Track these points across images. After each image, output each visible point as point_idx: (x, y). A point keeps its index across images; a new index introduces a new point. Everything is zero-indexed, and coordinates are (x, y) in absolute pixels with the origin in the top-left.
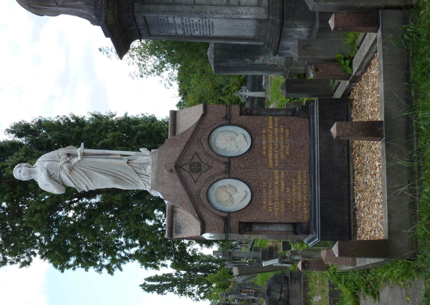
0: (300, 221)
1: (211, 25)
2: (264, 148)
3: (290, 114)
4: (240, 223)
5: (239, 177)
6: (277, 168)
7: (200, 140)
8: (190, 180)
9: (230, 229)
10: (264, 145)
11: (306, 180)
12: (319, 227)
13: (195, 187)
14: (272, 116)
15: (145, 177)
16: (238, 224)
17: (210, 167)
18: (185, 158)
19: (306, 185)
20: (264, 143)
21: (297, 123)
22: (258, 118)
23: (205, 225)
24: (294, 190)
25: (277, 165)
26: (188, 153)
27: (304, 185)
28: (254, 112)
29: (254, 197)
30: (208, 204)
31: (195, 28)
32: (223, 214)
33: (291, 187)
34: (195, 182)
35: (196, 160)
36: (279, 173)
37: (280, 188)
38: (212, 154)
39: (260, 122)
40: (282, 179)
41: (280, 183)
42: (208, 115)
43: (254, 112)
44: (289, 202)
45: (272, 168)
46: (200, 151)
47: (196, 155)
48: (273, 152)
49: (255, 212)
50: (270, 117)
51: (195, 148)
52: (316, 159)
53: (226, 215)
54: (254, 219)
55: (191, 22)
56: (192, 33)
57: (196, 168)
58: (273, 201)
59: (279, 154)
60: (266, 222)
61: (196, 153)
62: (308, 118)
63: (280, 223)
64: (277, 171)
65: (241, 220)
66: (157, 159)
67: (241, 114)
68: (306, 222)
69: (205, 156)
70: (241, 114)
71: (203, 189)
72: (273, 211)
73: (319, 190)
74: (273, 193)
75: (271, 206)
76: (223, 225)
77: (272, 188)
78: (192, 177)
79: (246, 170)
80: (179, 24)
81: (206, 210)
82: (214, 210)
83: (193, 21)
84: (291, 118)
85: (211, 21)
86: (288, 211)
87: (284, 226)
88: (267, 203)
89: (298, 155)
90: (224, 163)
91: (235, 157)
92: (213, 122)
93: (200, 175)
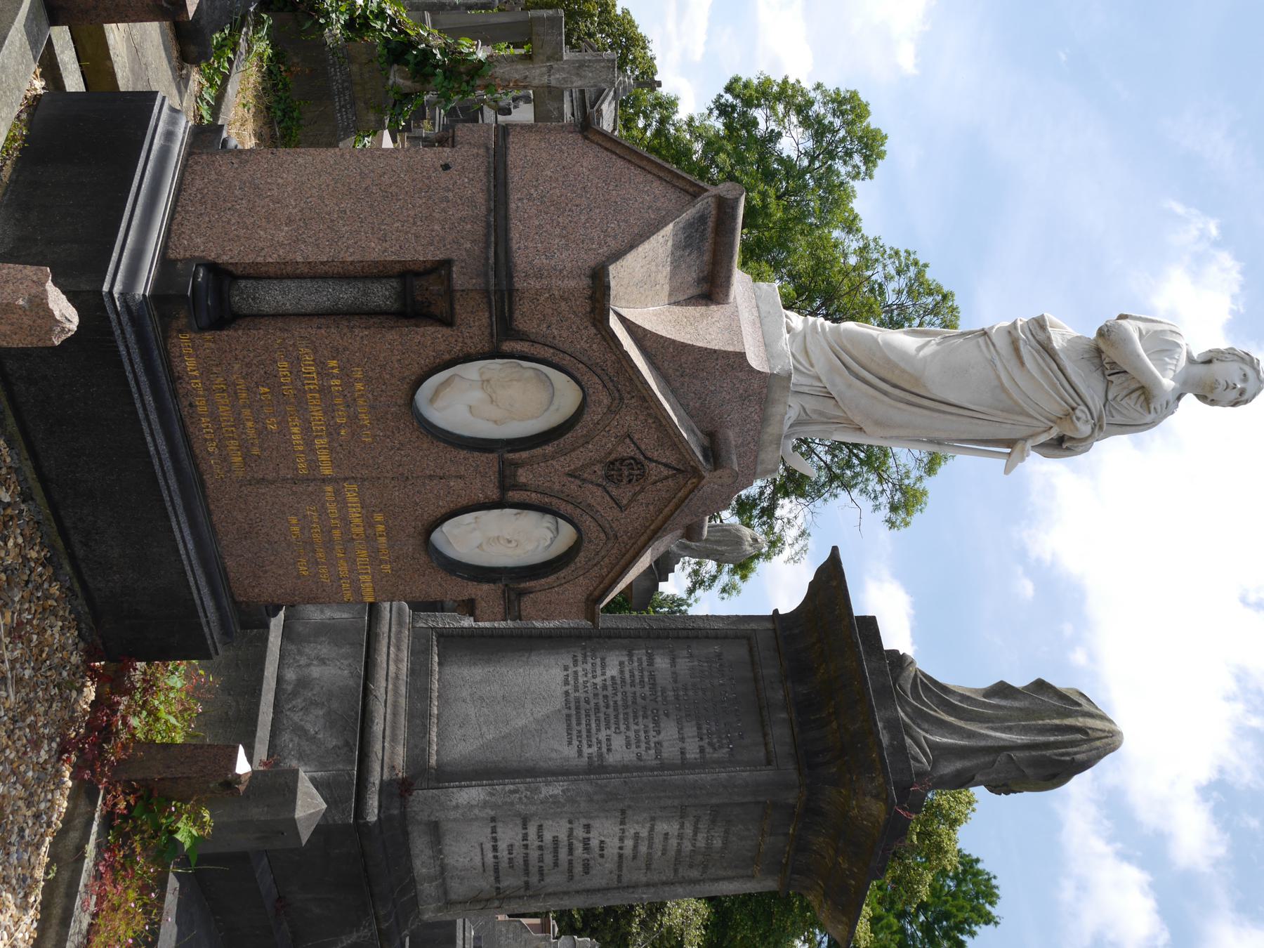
0: (208, 336)
1: (574, 722)
7: (608, 539)
9: (489, 302)
11: (209, 454)
12: (118, 332)
15: (806, 389)
16: (458, 321)
18: (664, 494)
19: (206, 440)
23: (593, 310)
24: (249, 424)
25: (329, 489)
26: (651, 507)
27: (212, 440)
30: (579, 376)
31: (619, 698)
32: (519, 346)
33: (262, 432)
36: (314, 465)
39: (401, 588)
40: (302, 452)
41: (309, 444)
44: (263, 390)
47: (625, 502)
48: (346, 521)
49: (394, 359)
52: (183, 518)
53: (507, 346)
55: (632, 734)
56: (625, 659)
58: (324, 391)
62: (235, 602)
64: (327, 472)
66: (762, 456)
68: (180, 331)
69: (592, 501)
71: (596, 418)
72: (321, 365)
73: (149, 439)
74: (329, 410)
76: (517, 314)
77: (332, 432)
78: (638, 448)
80: (667, 715)
81: (585, 359)
82: (555, 360)
83: (628, 745)
85: (575, 743)
87: (266, 308)
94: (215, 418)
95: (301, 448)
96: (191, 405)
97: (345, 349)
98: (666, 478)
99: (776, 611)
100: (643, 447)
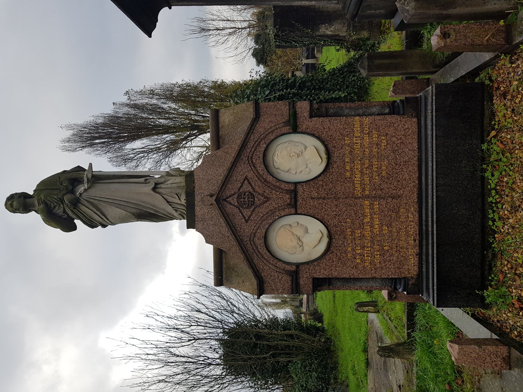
2: (348, 168)
3: (387, 111)
4: (314, 279)
5: (311, 212)
6: (368, 197)
7: (251, 158)
8: (238, 220)
10: (348, 162)
13: (246, 229)
14: (359, 115)
17: (268, 199)
19: (412, 221)
20: (347, 160)
21: (398, 125)
22: (338, 121)
23: (263, 283)
25: (367, 193)
26: (235, 179)
27: (410, 221)
28: (331, 111)
29: (334, 240)
30: (267, 253)
32: (288, 268)
33: (389, 225)
34: (247, 221)
35: (247, 188)
36: (372, 205)
37: (372, 226)
38: (270, 178)
39: (342, 127)
41: (372, 218)
42: (262, 119)
43: (331, 111)
44: (386, 248)
45: (360, 197)
46: (250, 175)
47: (246, 182)
49: (335, 263)
50: (357, 118)
51: (243, 170)
53: (294, 268)
54: (335, 274)
57: (248, 201)
58: (363, 248)
59: (371, 175)
60: (352, 277)
61: (246, 178)
63: (373, 278)
64: (367, 202)
65: (315, 276)
67: (311, 116)
68: (412, 278)
70: (311, 116)
75: (360, 255)
78: (242, 213)
79: (321, 201)
81: (265, 261)
82: (276, 261)
84: (389, 118)
86: (385, 262)
88: (353, 250)
89: (401, 176)
90: (288, 192)
91: (303, 182)
92: (270, 131)
93: (254, 210)
94: (408, 235)
95: (375, 216)
96: (415, 240)
97: (353, 268)
98: (230, 196)
99: (170, 8)
100: (241, 214)
